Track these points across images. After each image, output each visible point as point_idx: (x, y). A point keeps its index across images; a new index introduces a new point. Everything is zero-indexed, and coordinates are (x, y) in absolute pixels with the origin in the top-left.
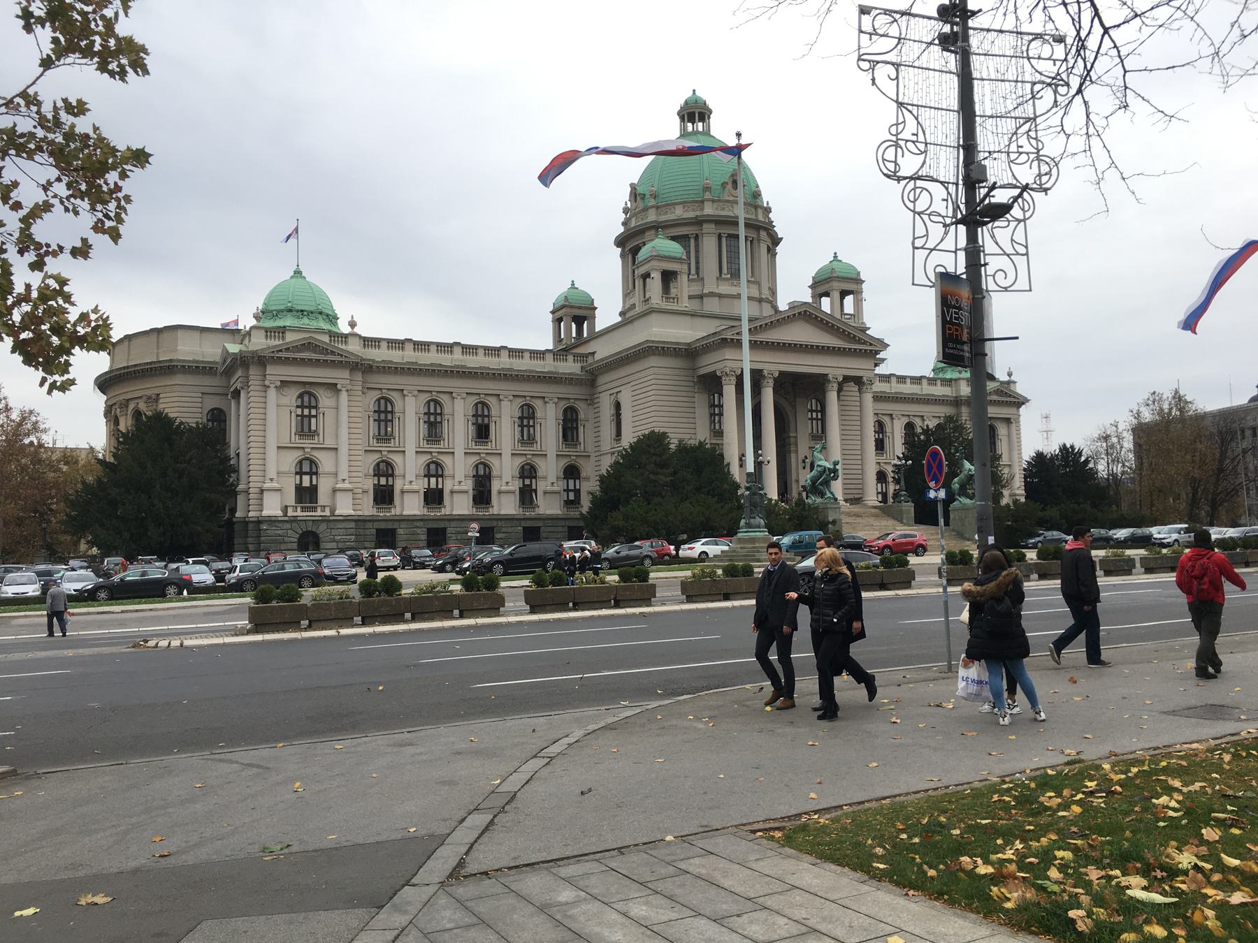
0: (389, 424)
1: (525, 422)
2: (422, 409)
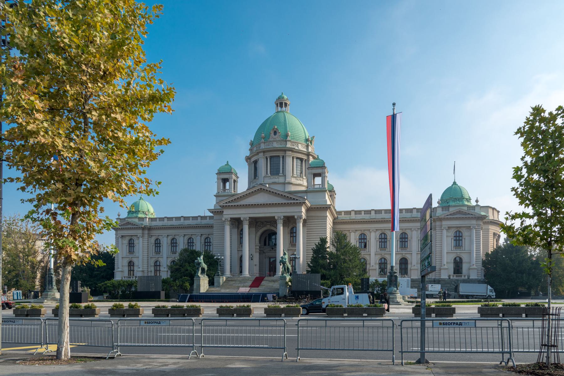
0: (461, 241)
1: (189, 244)
2: (453, 235)
